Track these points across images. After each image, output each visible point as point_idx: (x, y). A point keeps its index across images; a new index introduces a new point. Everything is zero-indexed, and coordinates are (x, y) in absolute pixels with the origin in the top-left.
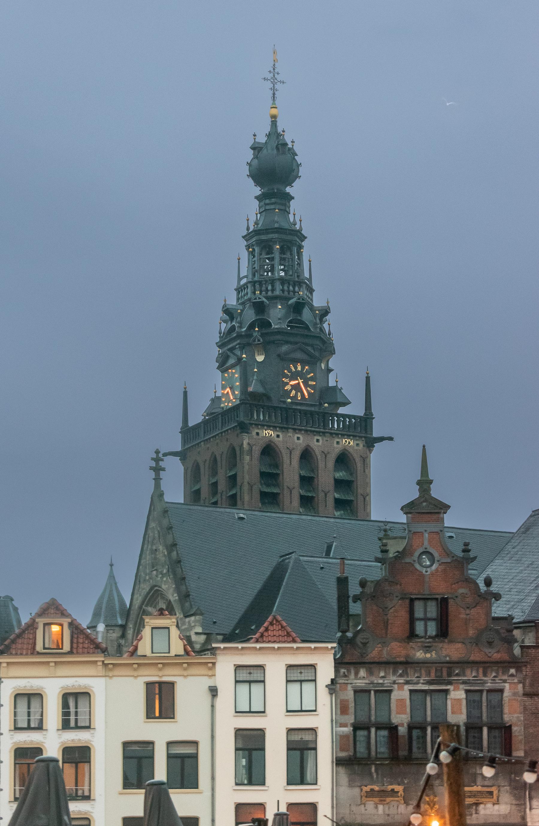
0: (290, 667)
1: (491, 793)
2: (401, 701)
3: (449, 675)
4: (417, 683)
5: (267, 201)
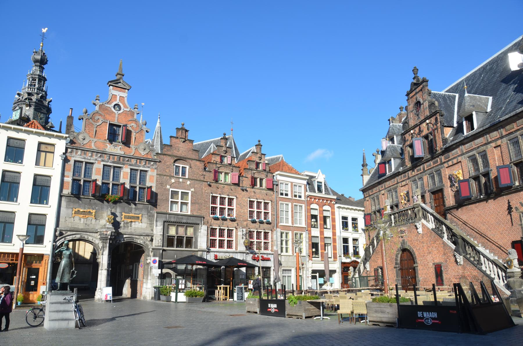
0: (40, 144)
1: (138, 218)
2: (98, 170)
3: (123, 161)
4: (108, 162)
5: (36, 67)
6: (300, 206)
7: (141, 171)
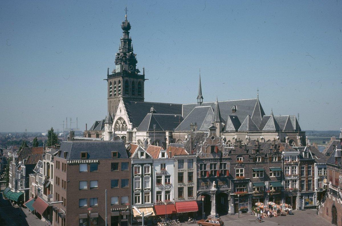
7: (224, 163)
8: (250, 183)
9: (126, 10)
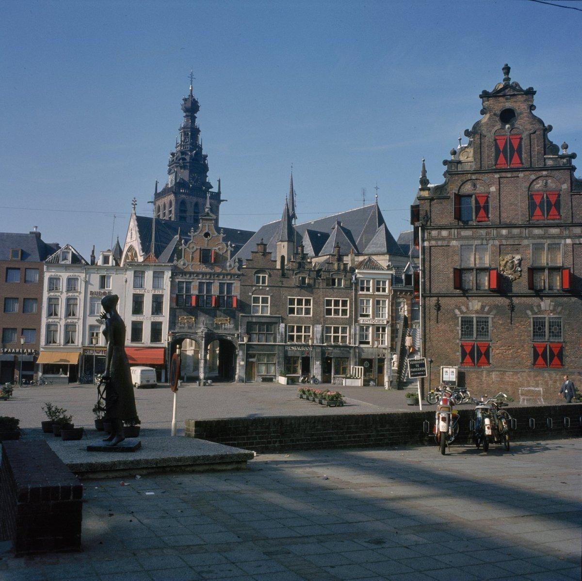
4: (202, 279)
6: (383, 301)
7: (228, 283)
8: (282, 325)
9: (192, 78)
